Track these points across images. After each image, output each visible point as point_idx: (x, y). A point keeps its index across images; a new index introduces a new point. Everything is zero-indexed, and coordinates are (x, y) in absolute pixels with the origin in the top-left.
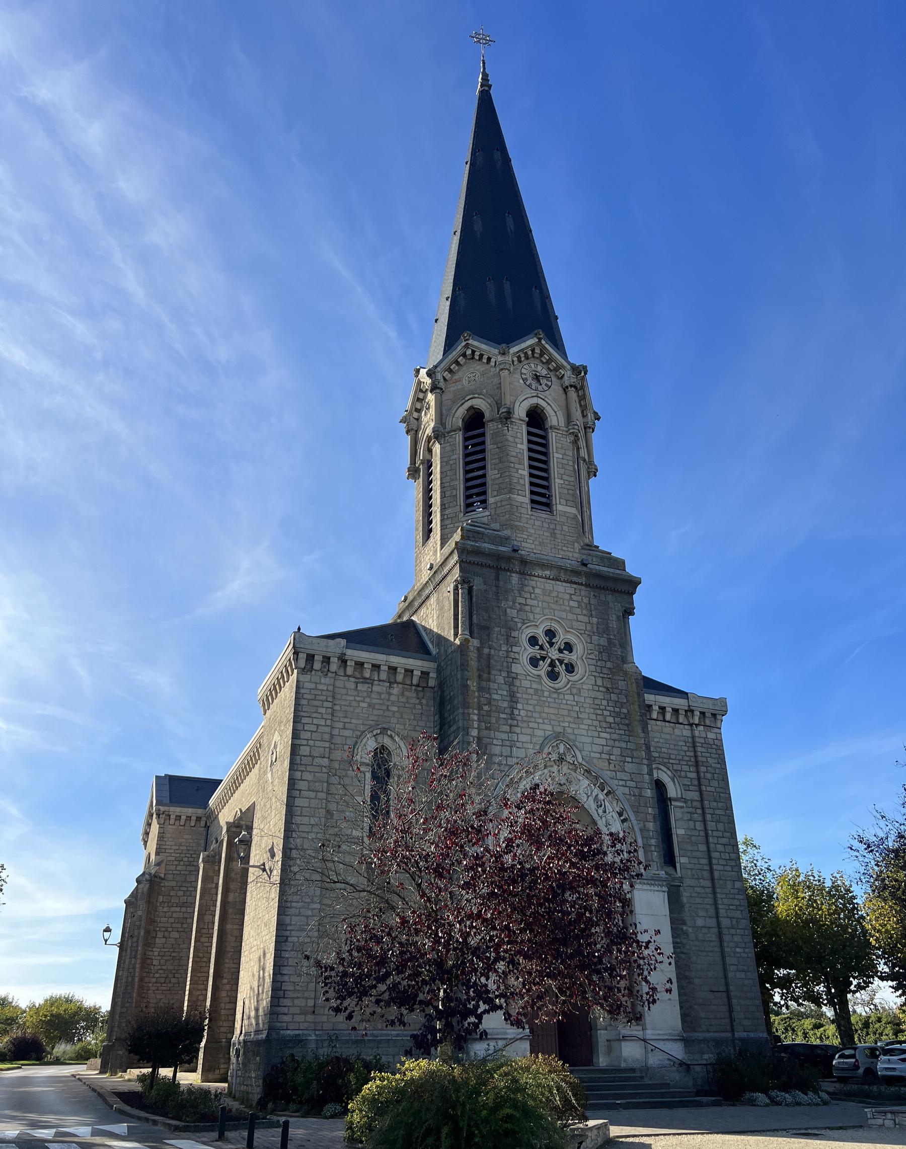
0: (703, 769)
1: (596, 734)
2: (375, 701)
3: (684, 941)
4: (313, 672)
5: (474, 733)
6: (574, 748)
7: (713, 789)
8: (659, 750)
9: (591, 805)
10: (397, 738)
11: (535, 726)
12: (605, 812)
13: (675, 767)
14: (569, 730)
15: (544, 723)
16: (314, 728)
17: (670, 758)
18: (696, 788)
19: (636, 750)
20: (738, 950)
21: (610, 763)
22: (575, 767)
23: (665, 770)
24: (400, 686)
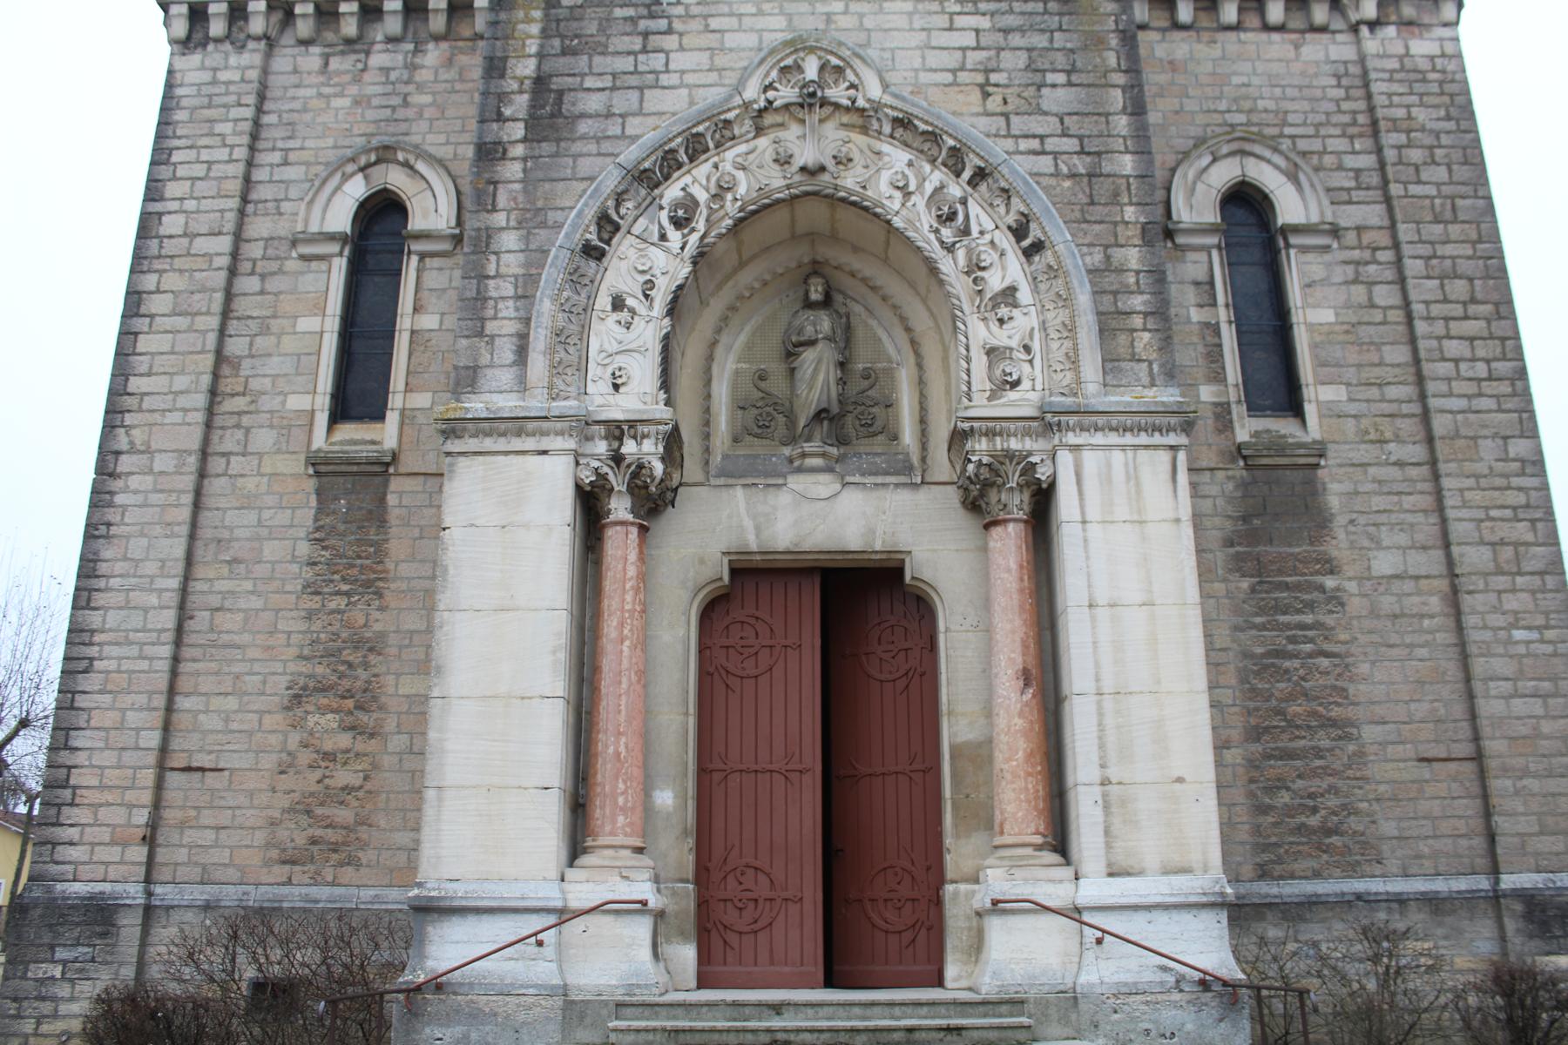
0: (1390, 139)
1: (943, 21)
2: (371, 90)
3: (1329, 620)
4: (210, 47)
5: (526, 68)
6: (857, 63)
7: (1433, 191)
8: (1247, 105)
9: (917, 220)
10: (421, 166)
11: (734, 22)
12: (966, 232)
13: (1302, 145)
14: (844, 22)
15: (760, 13)
16: (200, 170)
17: (1284, 123)
18: (1376, 195)
19: (1085, 48)
20: (1518, 634)
21: (986, 95)
22: (862, 117)
23: (1267, 153)
24: (444, 45)
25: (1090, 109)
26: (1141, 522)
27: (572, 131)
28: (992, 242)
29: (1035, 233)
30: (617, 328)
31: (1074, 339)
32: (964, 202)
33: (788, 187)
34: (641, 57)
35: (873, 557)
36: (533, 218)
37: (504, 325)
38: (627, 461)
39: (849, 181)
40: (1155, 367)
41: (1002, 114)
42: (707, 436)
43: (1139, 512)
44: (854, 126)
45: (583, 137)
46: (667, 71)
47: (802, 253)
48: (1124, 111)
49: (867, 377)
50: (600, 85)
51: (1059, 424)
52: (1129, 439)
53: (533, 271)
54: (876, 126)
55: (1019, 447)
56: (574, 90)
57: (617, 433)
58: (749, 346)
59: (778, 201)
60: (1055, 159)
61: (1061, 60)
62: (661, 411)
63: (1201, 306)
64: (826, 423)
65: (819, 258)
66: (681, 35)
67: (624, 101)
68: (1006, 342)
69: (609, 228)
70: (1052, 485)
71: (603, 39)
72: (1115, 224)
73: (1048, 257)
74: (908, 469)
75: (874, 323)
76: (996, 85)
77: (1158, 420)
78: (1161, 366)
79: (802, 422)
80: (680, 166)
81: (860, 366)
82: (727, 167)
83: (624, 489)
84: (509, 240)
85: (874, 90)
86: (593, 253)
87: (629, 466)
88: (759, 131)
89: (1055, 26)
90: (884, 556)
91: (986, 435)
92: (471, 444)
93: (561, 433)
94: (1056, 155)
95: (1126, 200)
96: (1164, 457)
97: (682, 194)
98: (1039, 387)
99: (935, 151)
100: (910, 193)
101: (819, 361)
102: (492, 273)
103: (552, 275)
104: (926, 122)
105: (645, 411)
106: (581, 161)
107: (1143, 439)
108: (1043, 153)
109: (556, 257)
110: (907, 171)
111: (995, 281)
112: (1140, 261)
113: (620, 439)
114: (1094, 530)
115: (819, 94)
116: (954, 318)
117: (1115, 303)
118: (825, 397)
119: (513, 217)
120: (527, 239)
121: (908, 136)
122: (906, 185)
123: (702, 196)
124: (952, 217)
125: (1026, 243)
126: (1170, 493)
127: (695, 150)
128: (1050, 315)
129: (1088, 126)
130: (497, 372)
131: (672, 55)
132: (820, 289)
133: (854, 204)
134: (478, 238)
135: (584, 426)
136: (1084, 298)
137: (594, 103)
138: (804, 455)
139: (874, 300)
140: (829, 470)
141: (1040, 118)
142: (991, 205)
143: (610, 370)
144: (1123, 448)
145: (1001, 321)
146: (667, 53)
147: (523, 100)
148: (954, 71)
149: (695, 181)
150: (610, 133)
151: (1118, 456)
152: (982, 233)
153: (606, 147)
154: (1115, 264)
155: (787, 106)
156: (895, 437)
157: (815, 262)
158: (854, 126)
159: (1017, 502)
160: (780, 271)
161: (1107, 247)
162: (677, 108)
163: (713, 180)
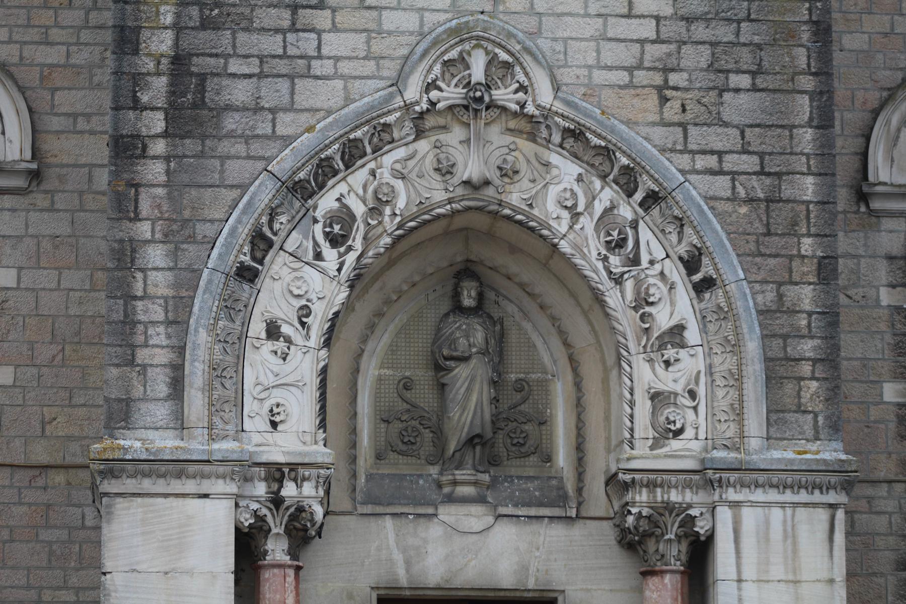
5: (161, 43)
6: (527, 60)
9: (585, 245)
19: (774, 43)
22: (531, 125)
25: (773, 120)
26: (796, 582)
27: (218, 126)
28: (662, 273)
29: (706, 269)
30: (272, 359)
31: (741, 389)
32: (634, 225)
33: (450, 201)
34: (290, 37)
35: (526, 595)
36: (180, 232)
37: (156, 354)
38: (286, 504)
39: (515, 197)
40: (821, 419)
41: (680, 124)
42: (353, 460)
43: (795, 573)
44: (521, 132)
45: (231, 135)
46: (320, 57)
47: (455, 252)
48: (809, 124)
49: (520, 390)
50: (247, 71)
51: (720, 480)
52: (788, 496)
53: (184, 293)
54: (544, 133)
55: (680, 499)
56: (218, 75)
57: (277, 475)
58: (393, 349)
59: (439, 217)
60: (733, 180)
61: (746, 57)
62: (321, 453)
63: (894, 287)
64: (478, 448)
65: (473, 257)
66: (334, 11)
67: (274, 92)
68: (670, 386)
69: (262, 246)
70: (711, 537)
71: (247, 11)
72: (791, 258)
73: (715, 298)
74: (562, 499)
75: (527, 326)
76: (676, 88)
77: (818, 478)
78: (827, 418)
79: (452, 446)
80: (336, 173)
81: (513, 377)
82: (385, 175)
83: (281, 531)
84: (156, 255)
85: (545, 96)
86: (247, 274)
87: (287, 508)
88: (420, 134)
89: (743, 15)
90: (536, 595)
91: (647, 486)
92: (130, 485)
93: (224, 477)
94: (734, 175)
95: (804, 230)
96: (823, 515)
97: (336, 205)
98: (702, 436)
99: (606, 167)
100: (579, 214)
101: (473, 380)
102: (140, 293)
103: (204, 303)
104: (599, 136)
105: (306, 454)
106: (230, 165)
107: (803, 497)
108: (721, 172)
109: (210, 282)
110: (576, 188)
111: (663, 319)
112: (814, 301)
113: (280, 482)
114: (749, 589)
115: (487, 99)
116: (619, 357)
117: (785, 348)
118: (478, 422)
119: (158, 228)
120: (174, 254)
121: (579, 148)
122: (575, 205)
123: (359, 209)
124: (621, 243)
125: (697, 277)
126: (826, 553)
127: (352, 156)
128: (717, 360)
129: (772, 141)
130: (152, 406)
131: (325, 37)
132: (473, 293)
133: (520, 223)
134: (122, 252)
135: (243, 469)
136: (752, 346)
137: (240, 93)
138: (455, 483)
139: (531, 306)
140: (481, 500)
141: (720, 130)
142: (663, 231)
143: (267, 405)
144: (782, 505)
145: (667, 363)
146: (319, 33)
147: (161, 83)
148: (630, 70)
149: (349, 191)
150: (259, 132)
151: (777, 514)
152: (652, 262)
153: (256, 148)
154: (788, 304)
155: (451, 108)
156: (548, 458)
157: (468, 261)
158: (521, 132)
159: (675, 552)
160: (430, 270)
161: (780, 284)
162: (331, 103)
163: (371, 190)
